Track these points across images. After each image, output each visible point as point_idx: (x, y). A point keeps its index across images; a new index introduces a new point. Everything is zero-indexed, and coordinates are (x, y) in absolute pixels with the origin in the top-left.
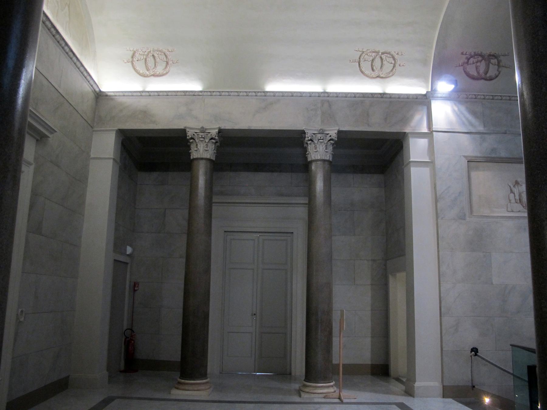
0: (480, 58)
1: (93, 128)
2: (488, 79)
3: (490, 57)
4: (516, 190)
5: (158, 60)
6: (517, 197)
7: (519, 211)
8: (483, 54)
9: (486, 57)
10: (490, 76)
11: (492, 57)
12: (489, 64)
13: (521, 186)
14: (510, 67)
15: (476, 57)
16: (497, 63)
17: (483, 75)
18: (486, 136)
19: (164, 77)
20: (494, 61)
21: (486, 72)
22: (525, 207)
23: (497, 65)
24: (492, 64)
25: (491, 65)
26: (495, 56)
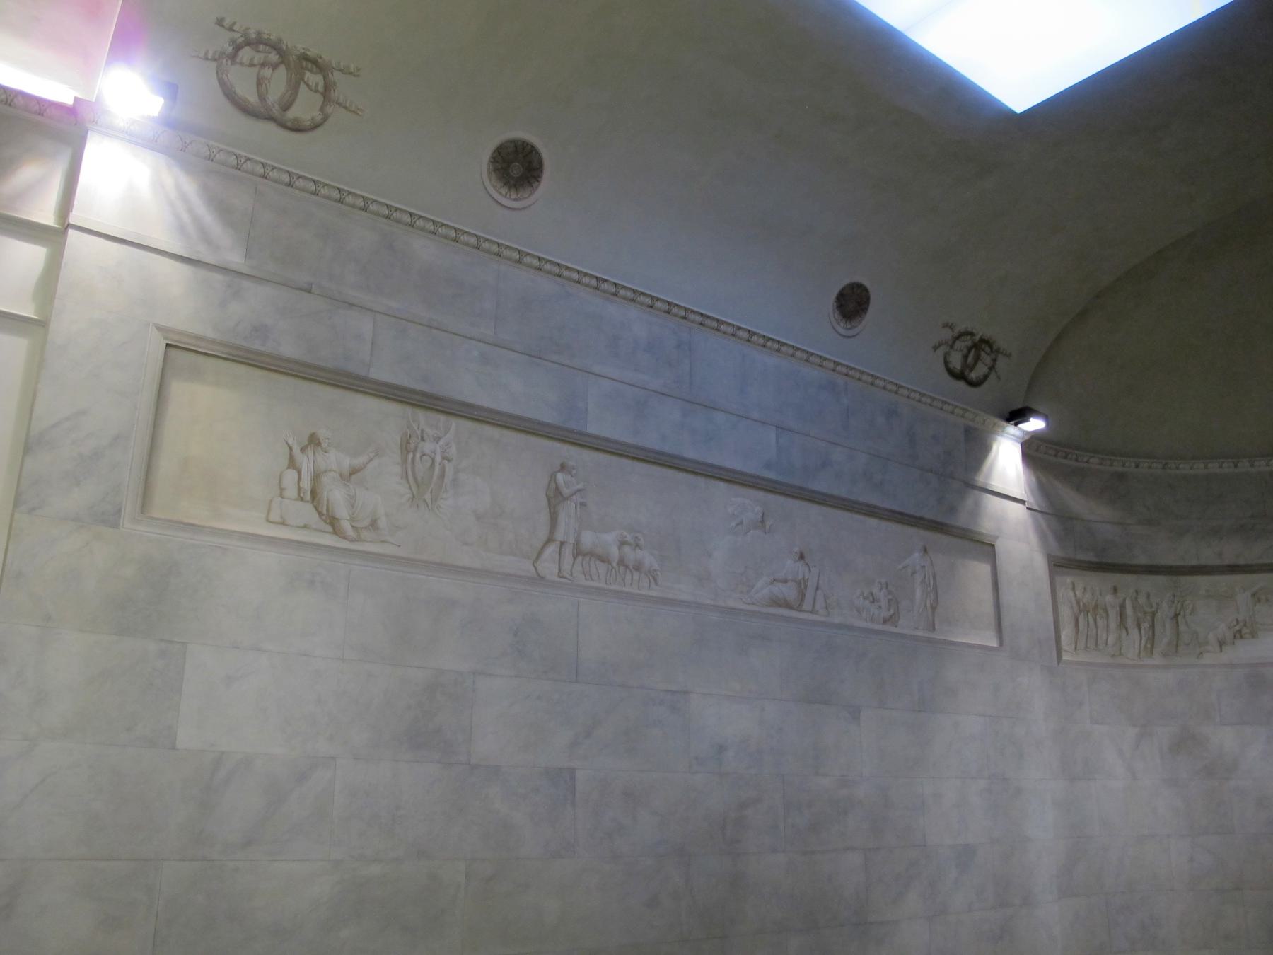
0: (274, 57)
2: (289, 124)
3: (304, 63)
4: (306, 463)
6: (306, 484)
7: (305, 527)
8: (284, 48)
9: (291, 59)
10: (296, 119)
11: (310, 65)
12: (299, 84)
13: (326, 452)
14: (359, 112)
15: (261, 47)
16: (321, 88)
17: (276, 111)
18: (246, 284)
20: (314, 78)
21: (286, 107)
22: (324, 517)
23: (322, 94)
24: (308, 85)
25: (303, 87)
26: (317, 64)
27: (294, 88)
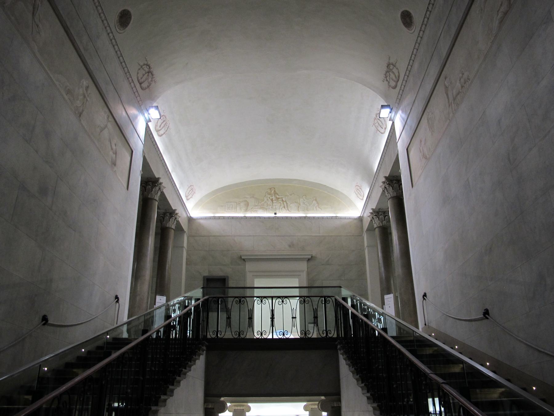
0: (388, 74)
3: (389, 68)
15: (387, 75)
16: (393, 66)
20: (391, 67)
27: (393, 73)
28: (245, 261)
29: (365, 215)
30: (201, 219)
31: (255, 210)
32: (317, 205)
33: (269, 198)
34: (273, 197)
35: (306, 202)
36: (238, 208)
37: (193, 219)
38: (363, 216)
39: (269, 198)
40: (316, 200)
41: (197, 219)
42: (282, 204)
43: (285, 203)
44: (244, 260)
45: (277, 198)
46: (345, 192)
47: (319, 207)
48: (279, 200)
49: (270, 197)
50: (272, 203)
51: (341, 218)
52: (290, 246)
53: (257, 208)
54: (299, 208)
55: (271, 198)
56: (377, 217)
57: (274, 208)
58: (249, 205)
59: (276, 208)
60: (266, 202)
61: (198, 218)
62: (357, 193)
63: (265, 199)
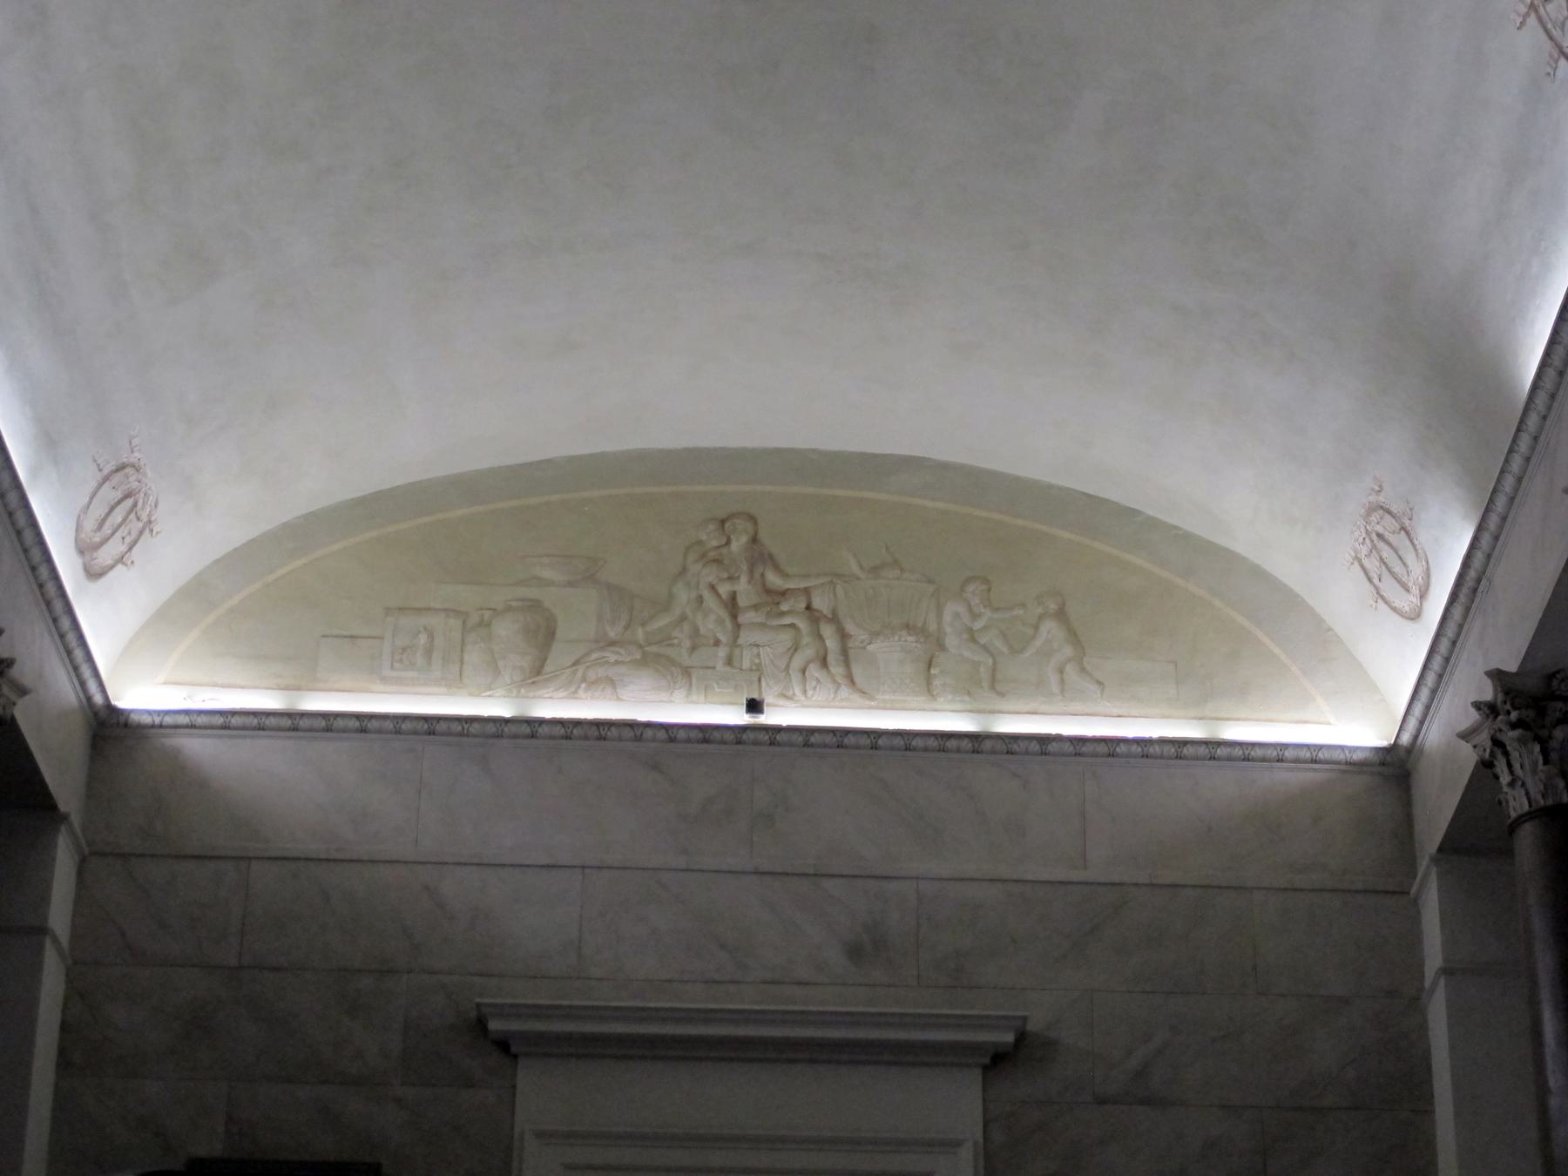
1: (1408, 893)
5: (1391, 538)
19: (1433, 580)
28: (515, 1057)
29: (1435, 736)
30: (192, 726)
31: (601, 672)
32: (1068, 651)
33: (713, 588)
34: (743, 586)
35: (986, 628)
36: (473, 656)
37: (126, 725)
38: (1416, 737)
39: (713, 588)
40: (1061, 615)
41: (161, 726)
42: (806, 640)
43: (828, 631)
44: (503, 1045)
45: (768, 592)
46: (1284, 565)
47: (1083, 670)
48: (784, 607)
49: (722, 580)
50: (729, 624)
51: (1247, 753)
52: (855, 952)
53: (617, 663)
54: (933, 671)
55: (724, 589)
56: (1529, 734)
57: (746, 664)
58: (559, 634)
59: (758, 671)
60: (683, 618)
61: (168, 720)
62: (1372, 564)
63: (683, 596)
